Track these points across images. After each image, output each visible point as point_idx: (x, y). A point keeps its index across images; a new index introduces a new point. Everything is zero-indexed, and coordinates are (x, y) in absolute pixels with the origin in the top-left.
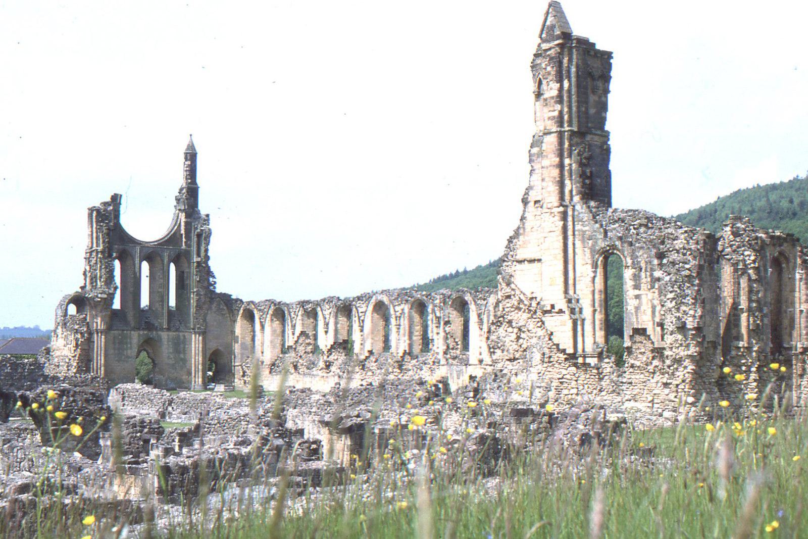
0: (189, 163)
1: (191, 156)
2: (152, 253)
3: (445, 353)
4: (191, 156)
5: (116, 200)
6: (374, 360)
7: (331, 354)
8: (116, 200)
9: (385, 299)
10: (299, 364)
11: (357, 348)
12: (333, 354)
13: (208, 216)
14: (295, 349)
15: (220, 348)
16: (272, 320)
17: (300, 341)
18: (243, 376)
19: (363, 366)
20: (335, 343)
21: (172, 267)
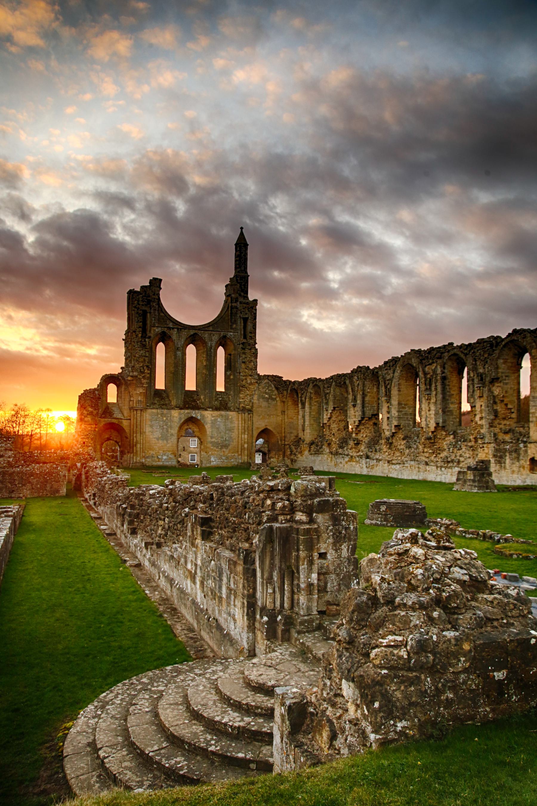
0: (238, 253)
1: (241, 246)
2: (195, 335)
3: (491, 425)
4: (241, 246)
5: (156, 283)
6: (402, 437)
7: (360, 431)
8: (156, 283)
9: (414, 362)
10: (332, 443)
11: (385, 426)
12: (362, 431)
13: (255, 301)
14: (329, 426)
15: (269, 428)
16: (311, 398)
17: (333, 419)
18: (291, 454)
19: (391, 444)
20: (363, 418)
21: (221, 351)
